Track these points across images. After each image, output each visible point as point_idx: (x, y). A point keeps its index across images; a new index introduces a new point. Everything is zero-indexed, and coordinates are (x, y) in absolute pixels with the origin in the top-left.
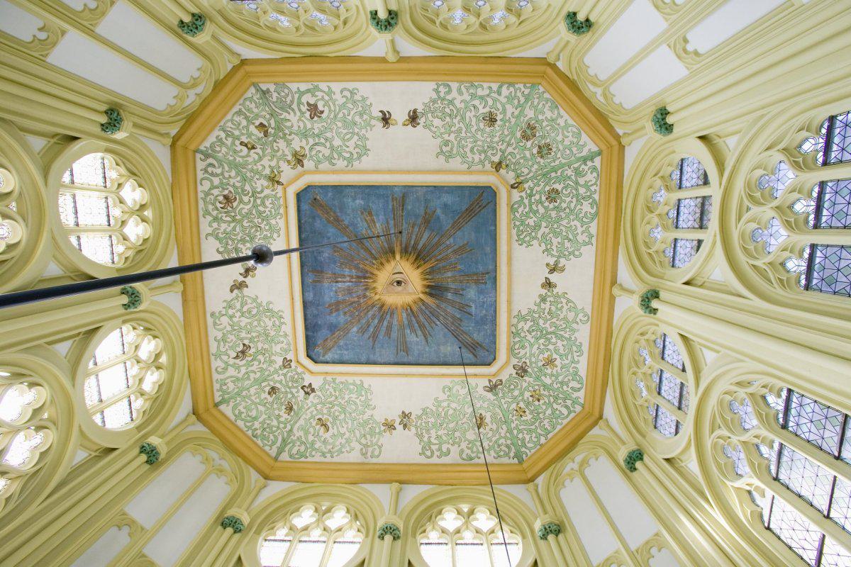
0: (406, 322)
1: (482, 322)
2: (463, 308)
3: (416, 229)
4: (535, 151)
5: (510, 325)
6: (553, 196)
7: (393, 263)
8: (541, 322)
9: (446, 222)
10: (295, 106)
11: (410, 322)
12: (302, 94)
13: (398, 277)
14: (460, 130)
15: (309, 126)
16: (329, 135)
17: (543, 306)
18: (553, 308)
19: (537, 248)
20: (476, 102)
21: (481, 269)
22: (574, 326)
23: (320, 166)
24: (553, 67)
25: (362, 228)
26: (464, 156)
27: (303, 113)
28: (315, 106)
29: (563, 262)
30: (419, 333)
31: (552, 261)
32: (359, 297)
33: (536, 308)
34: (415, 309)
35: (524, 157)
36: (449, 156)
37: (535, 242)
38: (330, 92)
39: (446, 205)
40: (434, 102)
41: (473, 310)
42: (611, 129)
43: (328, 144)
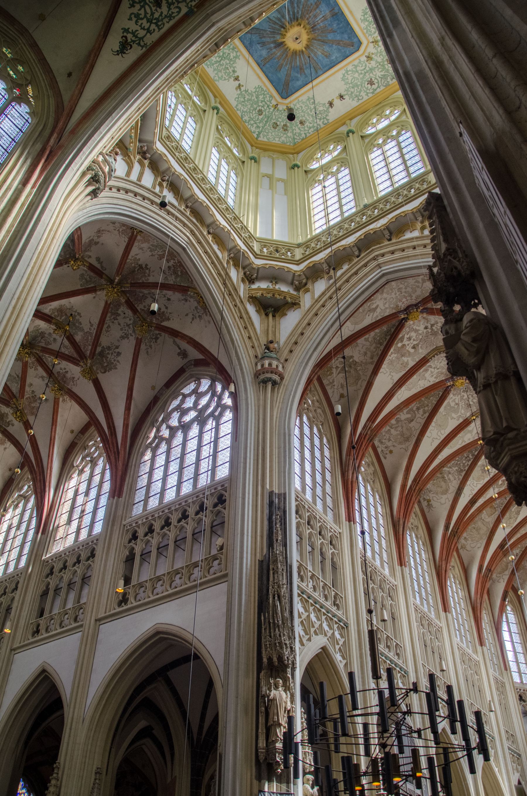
0: (283, 20)
1: (251, 44)
2: (263, 44)
3: (303, 63)
4: (278, 123)
5: (239, 51)
6: (260, 112)
7: (304, 45)
8: (228, 62)
9: (294, 74)
10: (380, 80)
11: (281, 22)
12: (378, 87)
13: (298, 41)
14: (311, 111)
15: (371, 75)
16: (361, 76)
17: (232, 69)
18: (228, 71)
19: (251, 89)
20: (311, 125)
21: (267, 65)
22: (216, 72)
23: (358, 61)
24: (293, 154)
25: (326, 48)
26: (303, 103)
27: (376, 79)
28: (371, 85)
29: (239, 92)
30: (274, 19)
31: (243, 89)
32: (310, 17)
33: (234, 65)
34: (282, 29)
35: (280, 118)
36: (309, 99)
37: (254, 90)
38: (367, 95)
39: (298, 80)
40: (327, 115)
41: (259, 46)
42: (260, 149)
43: (360, 72)
